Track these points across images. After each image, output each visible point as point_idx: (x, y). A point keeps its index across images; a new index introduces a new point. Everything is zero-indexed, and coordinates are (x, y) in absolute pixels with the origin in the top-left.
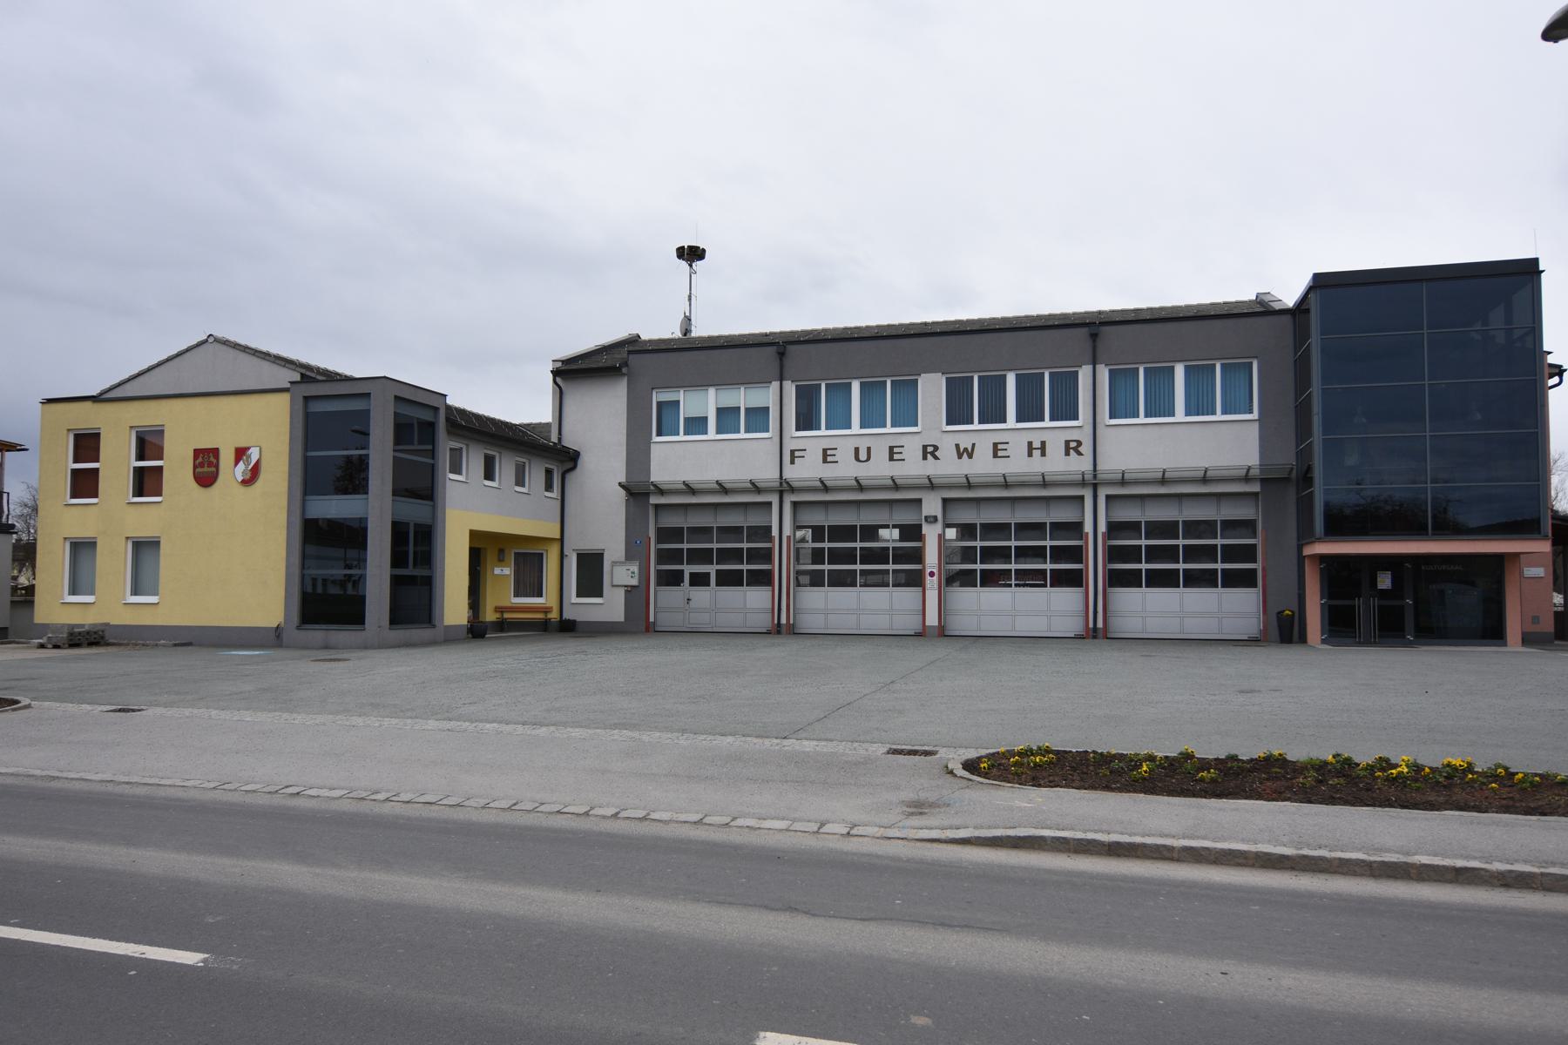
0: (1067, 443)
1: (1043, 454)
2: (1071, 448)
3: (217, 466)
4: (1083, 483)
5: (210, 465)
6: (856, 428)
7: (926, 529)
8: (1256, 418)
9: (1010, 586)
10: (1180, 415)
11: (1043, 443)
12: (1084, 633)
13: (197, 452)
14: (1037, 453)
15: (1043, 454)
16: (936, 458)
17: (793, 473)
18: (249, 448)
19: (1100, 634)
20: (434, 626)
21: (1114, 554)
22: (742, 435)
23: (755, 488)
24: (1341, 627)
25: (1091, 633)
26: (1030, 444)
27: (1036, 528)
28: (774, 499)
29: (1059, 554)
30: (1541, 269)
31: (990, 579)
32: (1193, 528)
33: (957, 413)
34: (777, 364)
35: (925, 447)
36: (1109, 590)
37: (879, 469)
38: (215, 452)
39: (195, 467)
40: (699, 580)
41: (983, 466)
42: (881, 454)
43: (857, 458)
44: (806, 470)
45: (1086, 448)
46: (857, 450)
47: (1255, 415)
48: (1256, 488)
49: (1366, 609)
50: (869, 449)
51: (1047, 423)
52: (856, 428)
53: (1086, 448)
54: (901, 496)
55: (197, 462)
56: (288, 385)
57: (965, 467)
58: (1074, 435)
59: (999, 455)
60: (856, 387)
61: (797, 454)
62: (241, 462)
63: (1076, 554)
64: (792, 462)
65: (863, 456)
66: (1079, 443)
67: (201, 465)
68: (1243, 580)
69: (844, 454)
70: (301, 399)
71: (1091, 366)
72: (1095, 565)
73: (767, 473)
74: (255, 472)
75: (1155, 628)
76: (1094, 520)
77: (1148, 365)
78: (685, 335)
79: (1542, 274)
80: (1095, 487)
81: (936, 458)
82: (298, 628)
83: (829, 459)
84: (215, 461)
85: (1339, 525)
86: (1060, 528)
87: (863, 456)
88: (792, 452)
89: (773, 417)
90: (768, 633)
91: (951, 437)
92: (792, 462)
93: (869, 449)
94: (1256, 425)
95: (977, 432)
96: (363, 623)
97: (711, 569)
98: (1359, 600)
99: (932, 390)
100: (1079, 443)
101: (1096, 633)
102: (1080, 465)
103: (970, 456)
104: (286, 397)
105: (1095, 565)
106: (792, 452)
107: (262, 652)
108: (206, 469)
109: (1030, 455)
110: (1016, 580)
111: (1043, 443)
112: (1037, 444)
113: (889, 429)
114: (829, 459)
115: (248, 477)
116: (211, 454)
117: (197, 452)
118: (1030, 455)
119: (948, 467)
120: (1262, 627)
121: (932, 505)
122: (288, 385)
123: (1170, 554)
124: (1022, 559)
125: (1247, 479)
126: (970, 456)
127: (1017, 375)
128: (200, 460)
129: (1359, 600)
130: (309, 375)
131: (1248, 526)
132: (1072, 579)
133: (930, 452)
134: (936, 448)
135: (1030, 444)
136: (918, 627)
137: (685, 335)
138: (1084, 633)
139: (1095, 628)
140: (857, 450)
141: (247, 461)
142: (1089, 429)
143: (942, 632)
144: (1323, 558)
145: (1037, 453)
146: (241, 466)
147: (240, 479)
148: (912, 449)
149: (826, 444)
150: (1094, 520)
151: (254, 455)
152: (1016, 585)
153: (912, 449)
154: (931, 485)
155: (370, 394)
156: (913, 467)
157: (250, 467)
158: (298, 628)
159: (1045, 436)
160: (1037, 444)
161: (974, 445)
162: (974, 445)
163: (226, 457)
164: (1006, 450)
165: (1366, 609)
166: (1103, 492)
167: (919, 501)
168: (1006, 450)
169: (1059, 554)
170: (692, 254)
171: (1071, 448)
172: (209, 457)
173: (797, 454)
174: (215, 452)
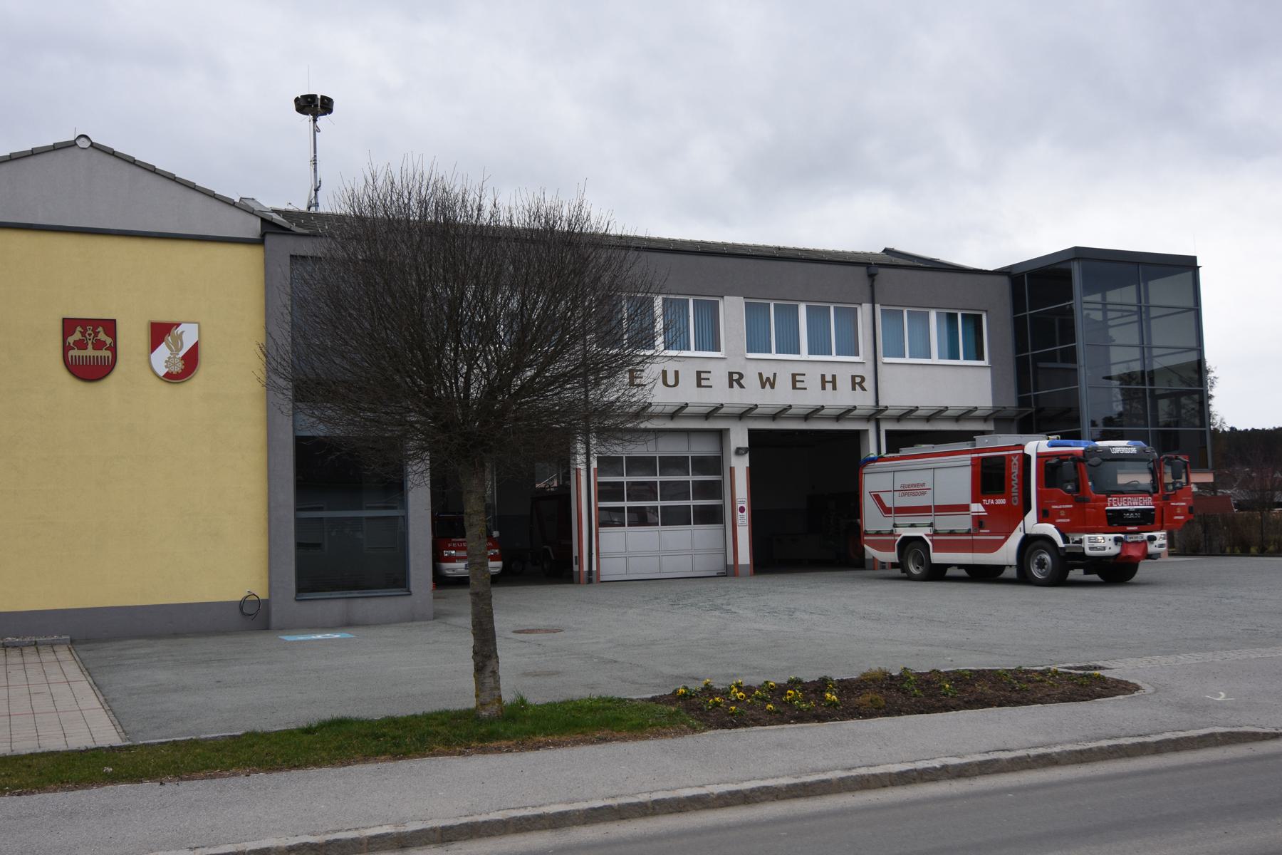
0: (853, 377)
3: (114, 349)
4: (868, 419)
5: (99, 345)
8: (987, 365)
11: (834, 377)
13: (69, 325)
16: (742, 386)
18: (178, 325)
26: (823, 376)
30: (1198, 265)
31: (641, 518)
33: (756, 342)
34: (867, 282)
35: (731, 374)
38: (110, 326)
39: (66, 349)
41: (782, 396)
43: (665, 383)
45: (869, 384)
46: (664, 373)
47: (985, 363)
50: (677, 373)
53: (869, 384)
55: (71, 340)
58: (858, 371)
59: (797, 386)
62: (163, 345)
65: (671, 381)
66: (863, 379)
67: (81, 345)
74: (191, 360)
78: (309, 208)
79: (1200, 268)
81: (742, 386)
84: (109, 341)
87: (671, 381)
90: (720, 575)
91: (753, 365)
93: (677, 373)
94: (989, 371)
99: (732, 312)
102: (863, 400)
103: (772, 386)
108: (90, 352)
109: (824, 388)
115: (178, 367)
116: (100, 329)
117: (69, 325)
118: (824, 388)
119: (752, 395)
128: (77, 336)
133: (735, 379)
134: (741, 376)
135: (823, 376)
137: (309, 208)
141: (176, 346)
146: (163, 352)
147: (162, 371)
148: (718, 377)
151: (188, 334)
153: (718, 377)
156: (720, 394)
157: (182, 354)
161: (775, 374)
162: (775, 374)
163: (132, 337)
166: (885, 426)
170: (313, 106)
171: (857, 383)
172: (96, 334)
174: (110, 326)
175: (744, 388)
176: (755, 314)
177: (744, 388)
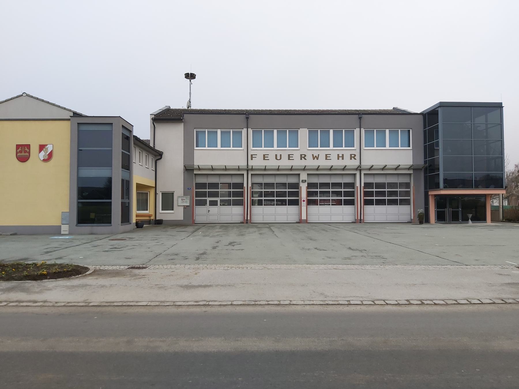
0: (351, 155)
1: (343, 159)
2: (352, 157)
3: (29, 153)
4: (356, 169)
5: (25, 152)
6: (275, 147)
7: (301, 185)
8: (411, 149)
9: (330, 205)
10: (387, 147)
11: (343, 155)
12: (355, 221)
13: (18, 146)
14: (341, 158)
15: (343, 159)
16: (305, 159)
17: (251, 163)
18: (47, 145)
19: (362, 221)
20: (131, 223)
21: (366, 194)
22: (231, 148)
23: (239, 169)
24: (441, 218)
25: (359, 221)
26: (338, 155)
27: (339, 185)
28: (245, 173)
29: (347, 194)
30: (503, 106)
32: (391, 185)
33: (312, 143)
35: (301, 155)
36: (365, 206)
37: (285, 163)
38: (28, 146)
39: (17, 153)
40: (213, 203)
41: (322, 162)
42: (322, 157)
43: (276, 159)
44: (257, 163)
45: (357, 157)
46: (276, 155)
47: (411, 148)
48: (411, 172)
49: (448, 211)
50: (281, 155)
51: (344, 148)
52: (275, 147)
53: (357, 157)
54: (294, 172)
55: (18, 151)
56: (70, 118)
57: (315, 163)
58: (353, 152)
59: (327, 159)
60: (331, 132)
61: (253, 156)
62: (43, 151)
63: (352, 194)
64: (252, 159)
65: (278, 158)
66: (355, 155)
67: (21, 152)
68: (406, 202)
69: (272, 157)
70: (77, 124)
71: (359, 129)
72: (359, 197)
73: (243, 163)
74: (50, 155)
75: (378, 219)
76: (359, 182)
77: (377, 129)
78: (188, 108)
79: (503, 107)
80: (360, 170)
81: (305, 159)
82: (77, 226)
83: (328, 158)
84: (28, 150)
85: (450, 184)
86: (347, 185)
87: (278, 158)
88: (252, 155)
89: (363, 140)
91: (310, 152)
92: (252, 159)
93: (281, 155)
94: (412, 151)
95: (319, 150)
96: (111, 223)
97: (218, 199)
98: (446, 209)
99: (303, 134)
100: (355, 155)
101: (359, 221)
102: (355, 163)
103: (317, 159)
104: (68, 123)
105: (359, 197)
106: (252, 155)
107: (73, 237)
108: (23, 154)
109: (338, 159)
110: (332, 203)
111: (343, 155)
112: (341, 155)
113: (288, 148)
114: (328, 158)
115: (46, 158)
116: (26, 147)
117: (18, 146)
118: (338, 159)
119: (310, 162)
120: (412, 218)
121: (304, 176)
122: (70, 118)
123: (383, 194)
124: (333, 196)
125: (409, 169)
126: (317, 159)
127: (333, 130)
128: (20, 149)
129: (446, 209)
130: (76, 115)
131: (408, 185)
132: (350, 203)
133: (303, 157)
134: (305, 156)
135: (338, 155)
136: (298, 220)
137: (188, 108)
138: (355, 221)
139: (361, 219)
140: (276, 155)
141: (46, 151)
142: (358, 151)
143: (361, 221)
144: (435, 196)
145: (341, 158)
146: (43, 153)
147: (42, 159)
148: (296, 156)
149: (276, 153)
150: (359, 182)
151: (50, 148)
152: (332, 205)
153: (296, 156)
154: (304, 169)
155: (112, 123)
156: (297, 162)
157: (48, 153)
158: (77, 226)
159: (343, 152)
160: (341, 155)
161: (319, 155)
162: (319, 155)
163: (34, 149)
164: (330, 157)
165: (448, 211)
166: (363, 172)
167: (299, 175)
168: (330, 157)
169: (347, 194)
170: (190, 76)
171: (352, 157)
172: (25, 149)
173: (253, 156)
174: (28, 146)
175: (306, 160)
176: (312, 134)
177: (306, 160)
